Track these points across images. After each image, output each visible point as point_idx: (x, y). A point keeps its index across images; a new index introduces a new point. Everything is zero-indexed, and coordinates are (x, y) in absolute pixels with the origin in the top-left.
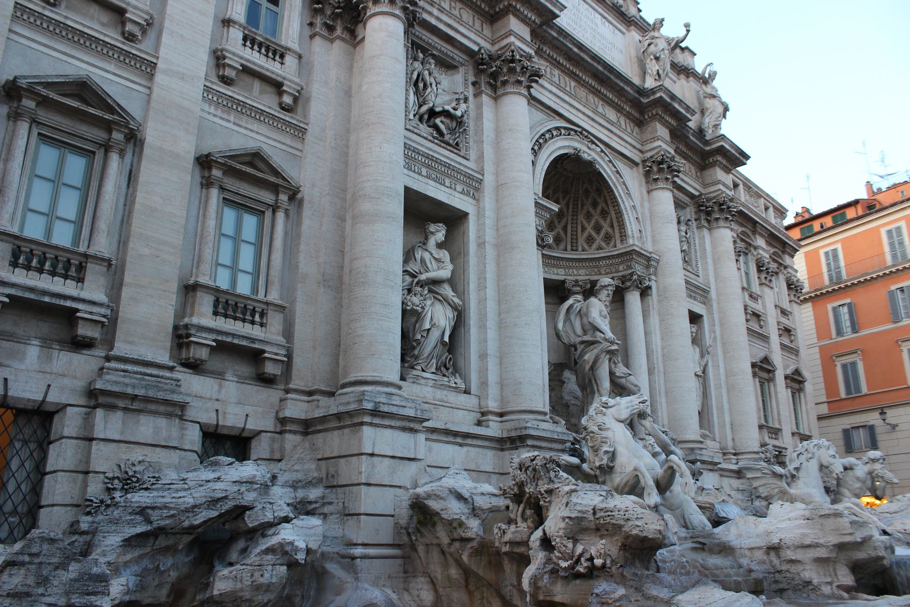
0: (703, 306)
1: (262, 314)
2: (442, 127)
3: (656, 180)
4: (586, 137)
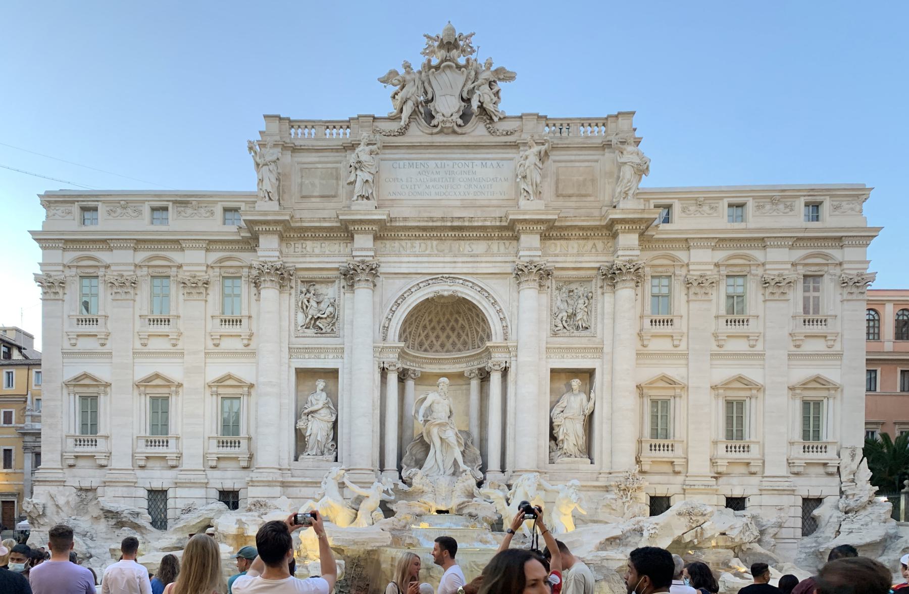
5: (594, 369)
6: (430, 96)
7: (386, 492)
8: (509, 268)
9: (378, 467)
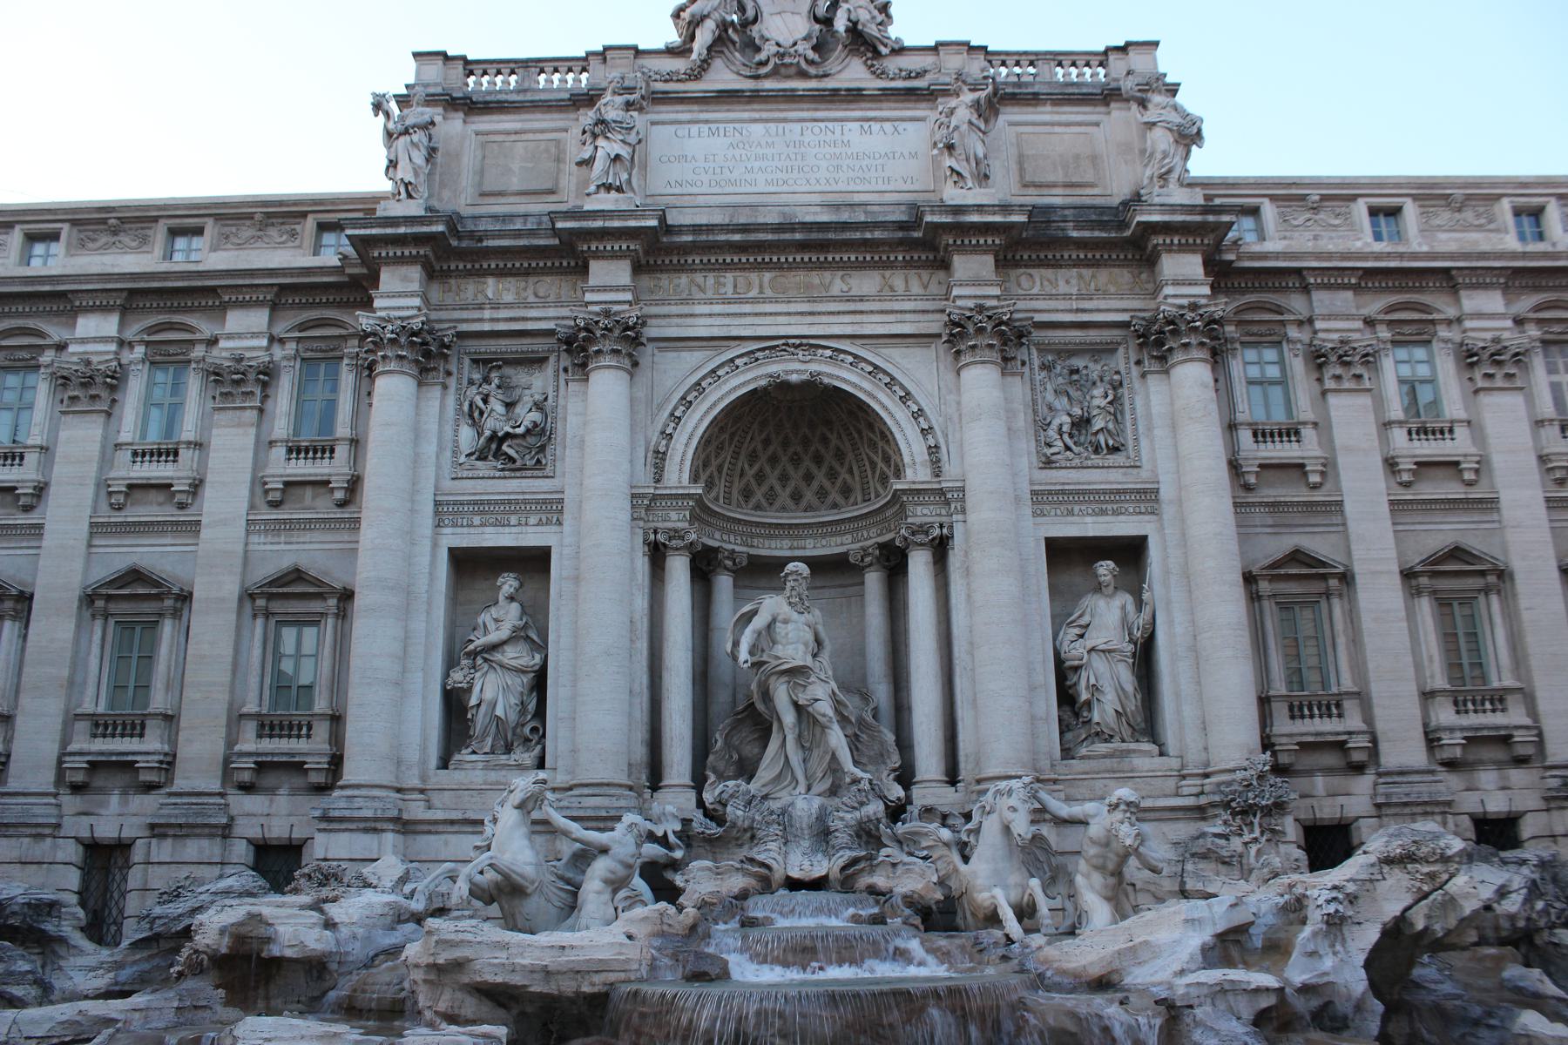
0: (1147, 518)
1: (310, 728)
2: (511, 452)
3: (958, 353)
5: (1145, 538)
6: (750, 13)
7: (663, 841)
8: (934, 324)
9: (644, 779)
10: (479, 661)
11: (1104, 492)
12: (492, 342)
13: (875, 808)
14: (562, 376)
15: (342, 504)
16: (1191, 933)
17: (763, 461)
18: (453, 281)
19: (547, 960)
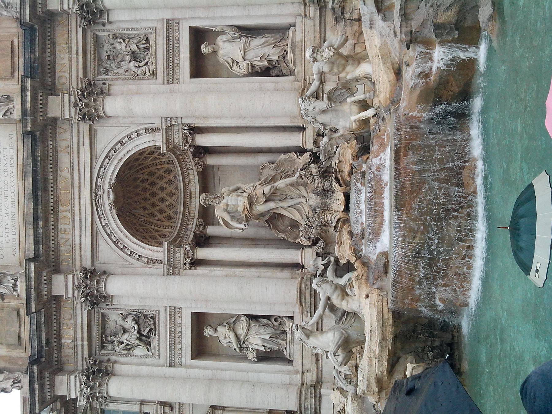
2: (147, 331)
3: (98, 117)
4: (96, 195)
7: (326, 266)
8: (85, 128)
10: (244, 346)
11: (168, 47)
12: (93, 340)
13: (314, 168)
14: (110, 306)
15: (171, 408)
16: (377, 25)
17: (153, 210)
18: (63, 359)
19: (377, 339)
